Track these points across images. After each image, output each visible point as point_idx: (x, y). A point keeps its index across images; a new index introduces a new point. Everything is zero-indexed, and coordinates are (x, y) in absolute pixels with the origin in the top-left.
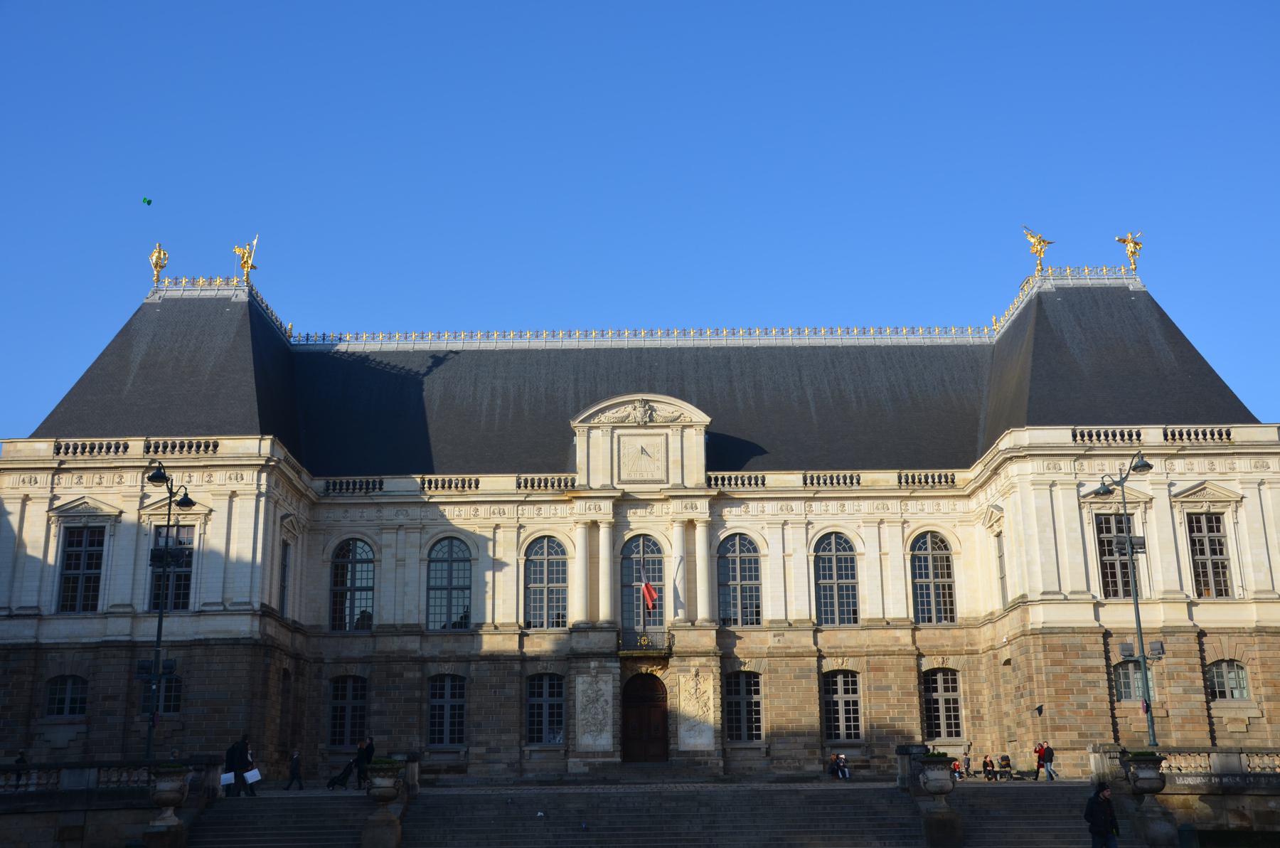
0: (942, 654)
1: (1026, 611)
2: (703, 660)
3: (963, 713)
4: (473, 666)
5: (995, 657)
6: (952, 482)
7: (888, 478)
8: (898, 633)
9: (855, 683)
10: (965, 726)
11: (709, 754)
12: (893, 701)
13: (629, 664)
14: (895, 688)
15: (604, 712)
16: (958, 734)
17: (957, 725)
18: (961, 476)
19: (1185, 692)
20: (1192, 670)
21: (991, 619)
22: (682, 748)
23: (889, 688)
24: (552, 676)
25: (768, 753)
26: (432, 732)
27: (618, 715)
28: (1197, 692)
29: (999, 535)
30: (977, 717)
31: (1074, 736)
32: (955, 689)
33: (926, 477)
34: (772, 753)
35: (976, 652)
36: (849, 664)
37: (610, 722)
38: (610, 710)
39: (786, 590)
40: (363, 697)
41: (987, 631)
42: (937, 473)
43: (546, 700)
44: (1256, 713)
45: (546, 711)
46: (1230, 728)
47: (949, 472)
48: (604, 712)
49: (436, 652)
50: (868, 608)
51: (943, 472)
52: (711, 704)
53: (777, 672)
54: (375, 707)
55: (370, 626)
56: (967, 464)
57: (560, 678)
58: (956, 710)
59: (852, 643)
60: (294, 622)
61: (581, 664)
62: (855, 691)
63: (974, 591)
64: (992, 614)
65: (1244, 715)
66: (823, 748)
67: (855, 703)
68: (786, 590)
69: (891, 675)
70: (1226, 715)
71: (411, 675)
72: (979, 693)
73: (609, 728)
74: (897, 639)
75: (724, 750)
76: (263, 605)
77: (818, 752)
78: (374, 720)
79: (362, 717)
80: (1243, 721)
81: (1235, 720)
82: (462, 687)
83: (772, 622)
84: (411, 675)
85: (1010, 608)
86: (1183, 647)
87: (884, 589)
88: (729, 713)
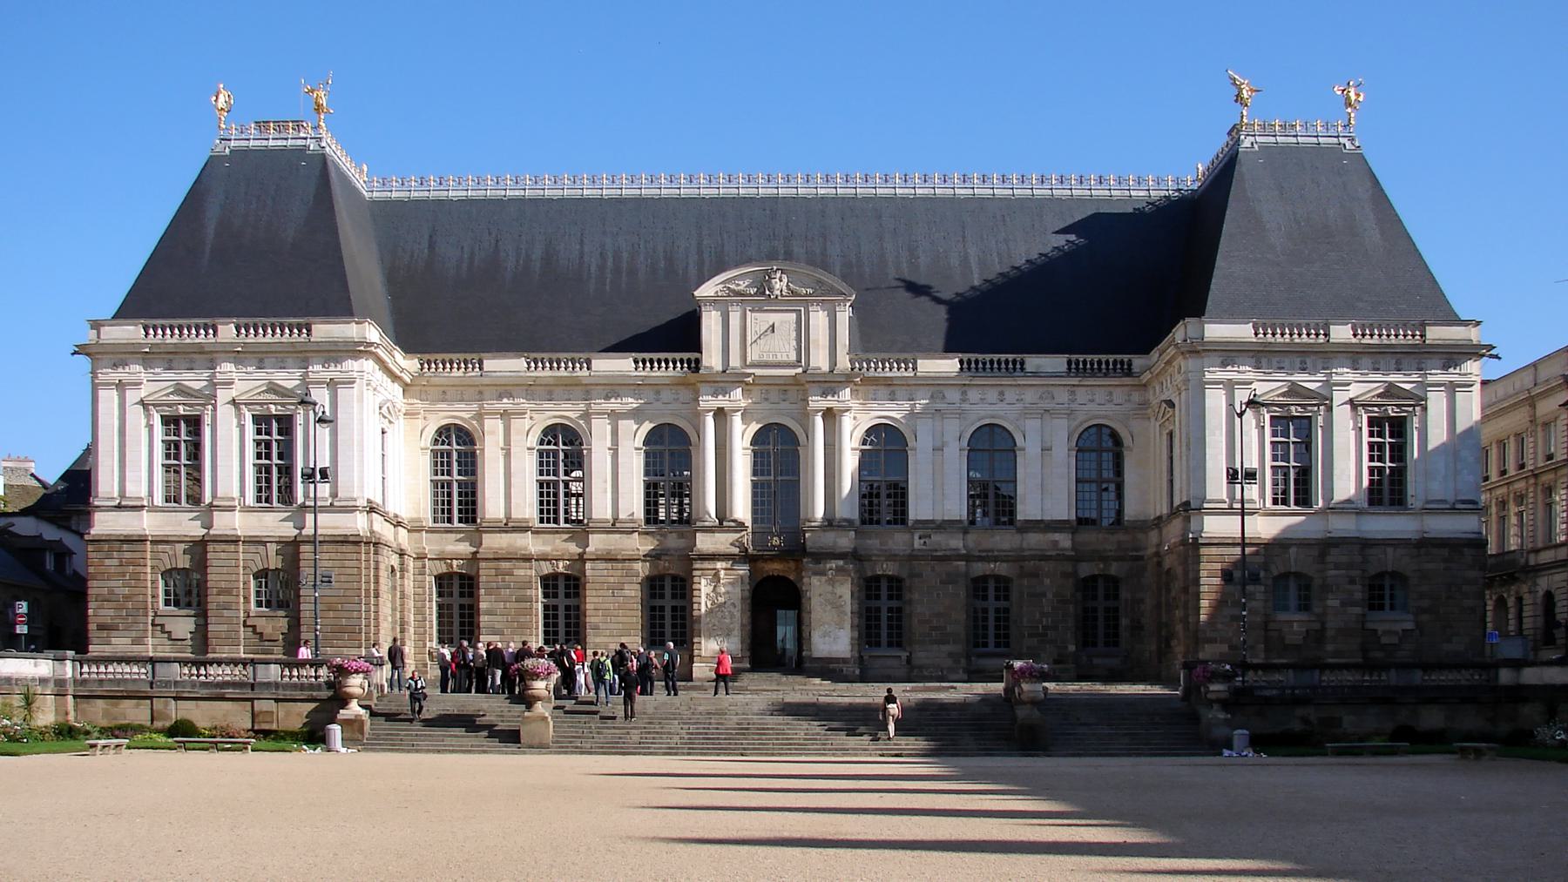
0: (1104, 559)
1: (1188, 519)
2: (841, 563)
3: (1124, 622)
4: (588, 565)
5: (1159, 564)
6: (1128, 371)
7: (1057, 362)
8: (1057, 536)
9: (1007, 589)
10: (1124, 634)
11: (844, 661)
12: (1048, 609)
13: (760, 565)
14: (1050, 596)
15: (732, 616)
16: (1116, 644)
17: (1117, 635)
18: (1138, 362)
19: (1343, 604)
20: (1352, 581)
21: (1159, 522)
22: (816, 654)
23: (1044, 595)
24: (674, 578)
25: (909, 660)
26: (546, 633)
27: (747, 620)
28: (1354, 604)
29: (1171, 434)
30: (1137, 627)
31: (1224, 648)
32: (1116, 597)
33: (1100, 362)
34: (915, 662)
35: (1141, 558)
36: (1002, 569)
37: (737, 626)
38: (738, 615)
39: (940, 491)
40: (471, 595)
41: (1153, 536)
42: (1111, 358)
43: (668, 603)
44: (1409, 626)
45: (668, 613)
46: (1384, 640)
47: (1126, 358)
48: (732, 616)
49: (547, 549)
50: (1027, 509)
51: (1119, 357)
52: (848, 609)
53: (920, 575)
54: (483, 606)
55: (474, 521)
56: (1146, 350)
57: (683, 580)
58: (1117, 619)
59: (1006, 546)
60: (396, 516)
61: (706, 565)
62: (1007, 598)
63: (1143, 496)
64: (1160, 518)
65: (1398, 627)
66: (968, 657)
67: (1007, 610)
68: (940, 491)
69: (1047, 581)
70: (1381, 628)
71: (522, 572)
72: (1142, 601)
73: (737, 632)
74: (1056, 543)
75: (861, 657)
76: (369, 501)
77: (963, 661)
78: (483, 619)
79: (471, 616)
80: (1396, 633)
81: (1388, 633)
82: (577, 587)
83: (917, 522)
84: (522, 572)
85: (1174, 513)
86: (1344, 559)
87: (1046, 489)
88: (868, 619)
